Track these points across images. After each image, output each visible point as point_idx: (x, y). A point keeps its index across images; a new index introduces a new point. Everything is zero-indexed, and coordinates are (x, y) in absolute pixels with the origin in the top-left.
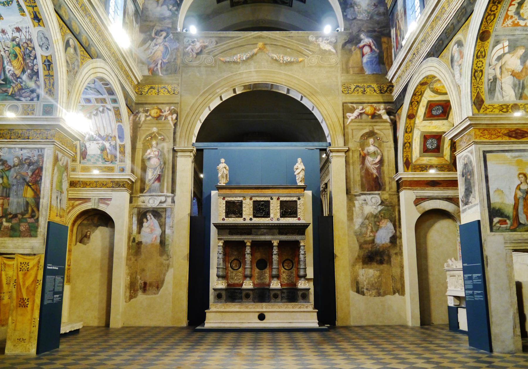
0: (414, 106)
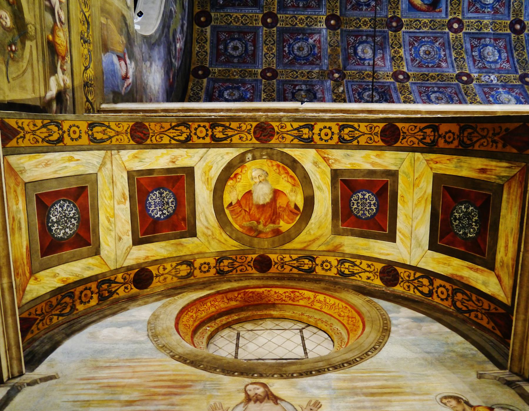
0: (172, 133)
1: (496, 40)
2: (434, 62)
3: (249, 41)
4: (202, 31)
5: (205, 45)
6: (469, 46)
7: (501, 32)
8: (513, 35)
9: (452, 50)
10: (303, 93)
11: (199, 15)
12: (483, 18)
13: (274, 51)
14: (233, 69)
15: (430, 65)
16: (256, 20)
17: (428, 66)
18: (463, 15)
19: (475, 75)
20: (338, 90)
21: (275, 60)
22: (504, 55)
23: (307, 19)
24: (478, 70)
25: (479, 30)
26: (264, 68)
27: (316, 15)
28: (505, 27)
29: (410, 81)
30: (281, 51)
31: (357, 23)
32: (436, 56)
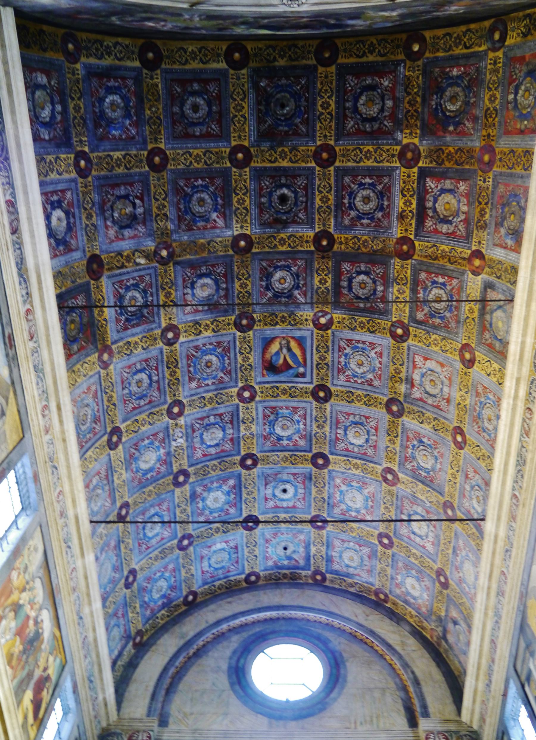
1: (232, 440)
2: (196, 372)
3: (208, 127)
4: (219, 55)
5: (197, 61)
6: (221, 411)
7: (242, 444)
8: (239, 458)
9: (215, 393)
10: (129, 210)
11: (243, 50)
12: (257, 424)
13: (196, 165)
14: (161, 107)
15: (192, 369)
16: (239, 137)
17: (189, 366)
18: (260, 402)
19: (182, 421)
20: (139, 257)
21: (182, 166)
22: (213, 451)
23: (244, 208)
24: (189, 423)
25: (243, 422)
26: (168, 152)
27: (251, 220)
28: (249, 448)
29: (165, 347)
30: (197, 174)
31: (243, 274)
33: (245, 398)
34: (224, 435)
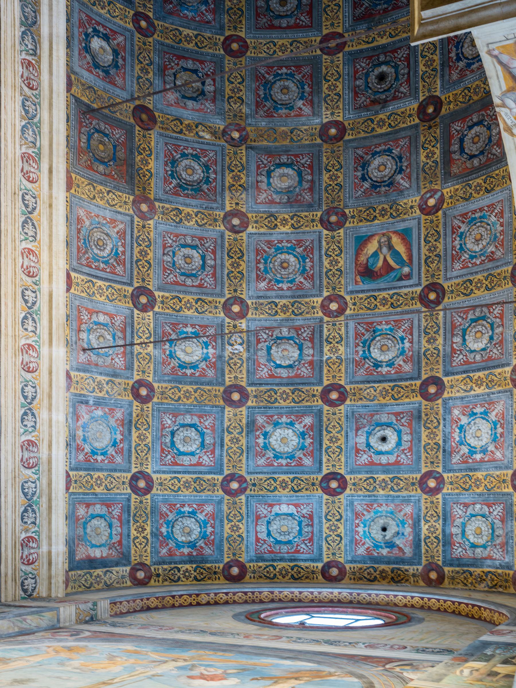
2: (266, 271)
6: (298, 323)
7: (325, 371)
9: (292, 300)
12: (347, 345)
15: (261, 266)
19: (243, 324)
22: (284, 373)
25: (327, 340)
28: (334, 377)
32: (279, 276)
33: (332, 311)
34: (300, 355)
